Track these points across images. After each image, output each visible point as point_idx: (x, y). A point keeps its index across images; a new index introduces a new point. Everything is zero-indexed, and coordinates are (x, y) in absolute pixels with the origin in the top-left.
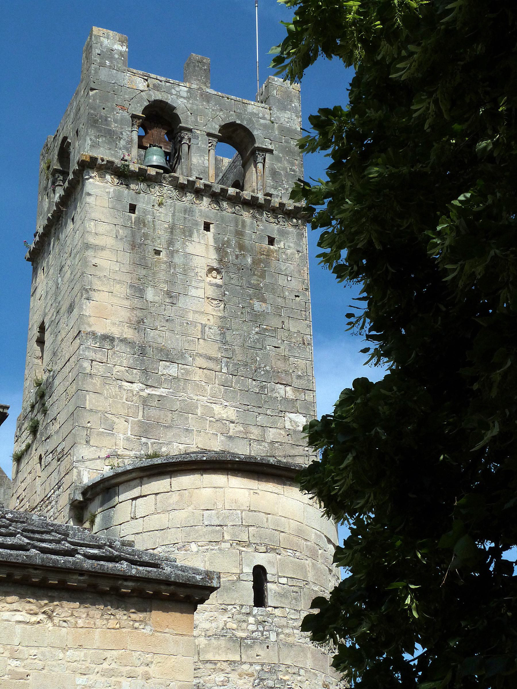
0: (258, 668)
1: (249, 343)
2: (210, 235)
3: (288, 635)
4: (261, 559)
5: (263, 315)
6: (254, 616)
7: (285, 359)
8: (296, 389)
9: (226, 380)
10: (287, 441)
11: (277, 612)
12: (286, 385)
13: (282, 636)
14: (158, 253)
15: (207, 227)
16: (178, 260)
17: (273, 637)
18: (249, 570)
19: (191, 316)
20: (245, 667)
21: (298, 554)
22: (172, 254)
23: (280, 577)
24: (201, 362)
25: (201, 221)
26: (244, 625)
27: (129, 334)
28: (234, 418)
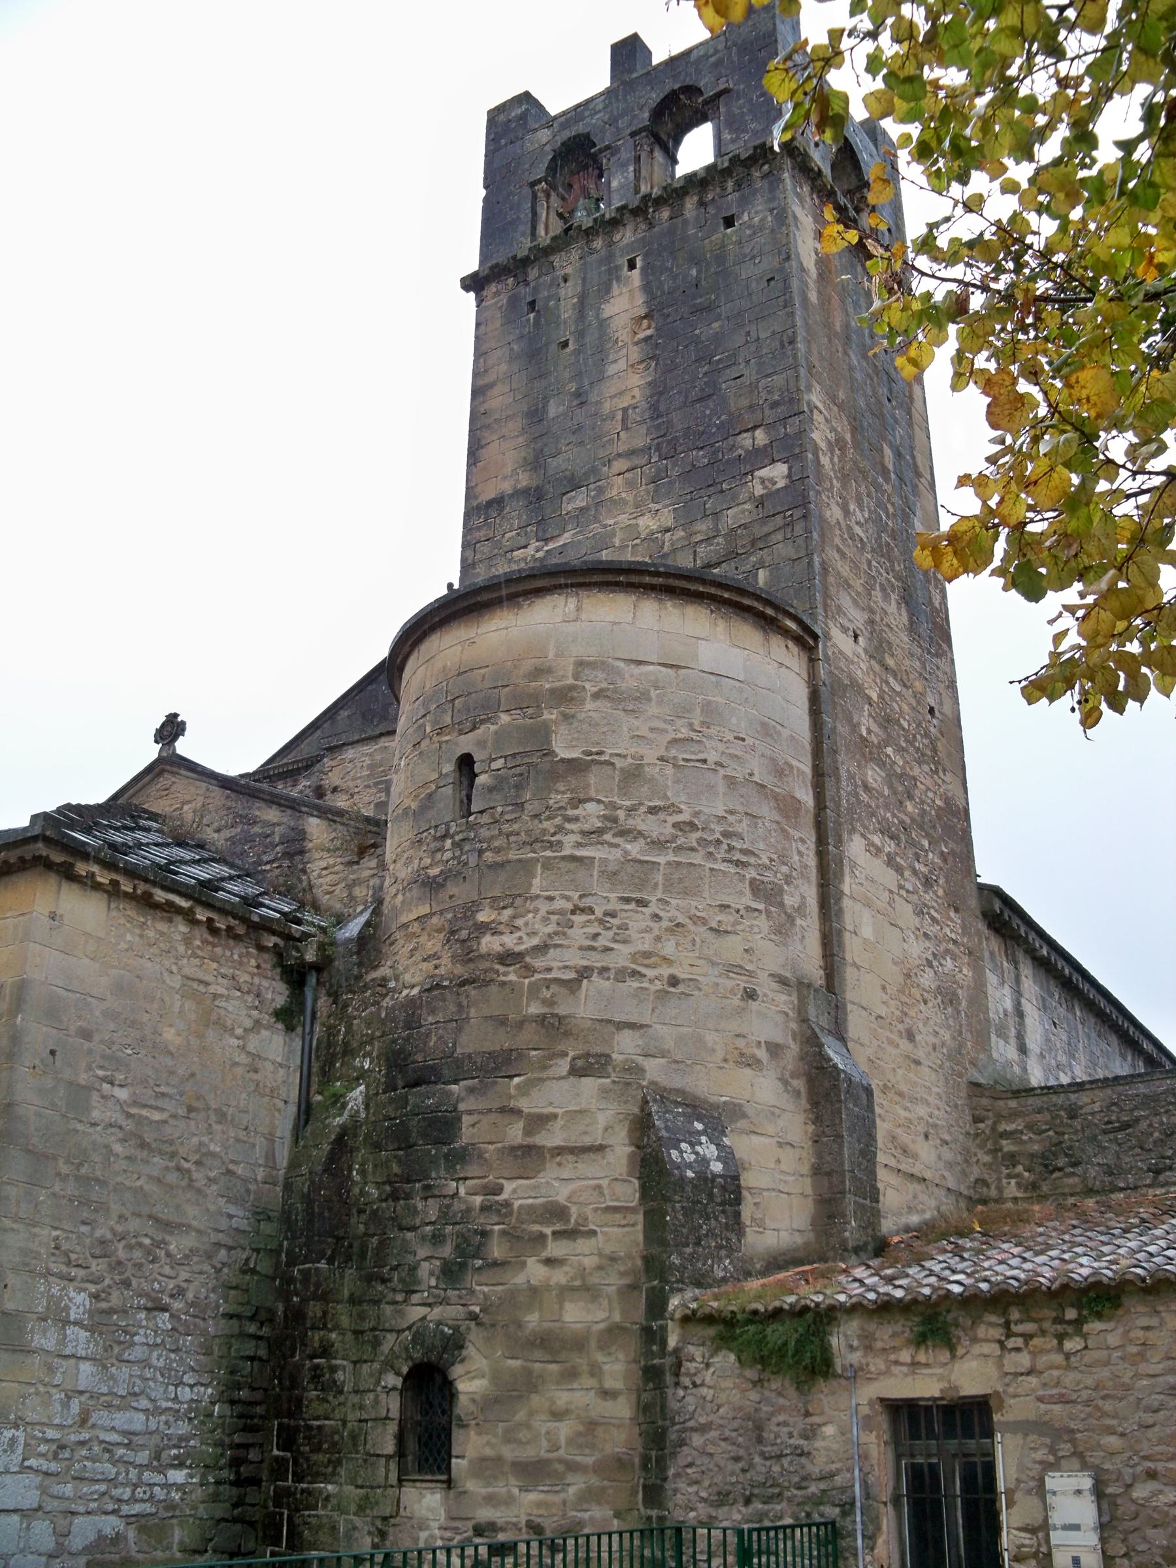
0: (450, 916)
1: (693, 395)
2: (636, 273)
3: (498, 850)
4: (466, 744)
5: (718, 338)
6: (452, 837)
7: (753, 387)
8: (769, 427)
9: (658, 470)
10: (755, 517)
11: (485, 819)
12: (755, 428)
13: (489, 856)
14: (565, 345)
15: (632, 265)
16: (591, 338)
17: (473, 860)
18: (449, 767)
19: (607, 407)
20: (435, 920)
21: (530, 711)
22: (580, 334)
23: (495, 760)
24: (620, 465)
25: (623, 262)
26: (439, 855)
27: (524, 480)
28: (669, 523)
